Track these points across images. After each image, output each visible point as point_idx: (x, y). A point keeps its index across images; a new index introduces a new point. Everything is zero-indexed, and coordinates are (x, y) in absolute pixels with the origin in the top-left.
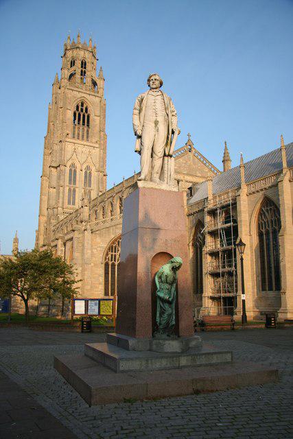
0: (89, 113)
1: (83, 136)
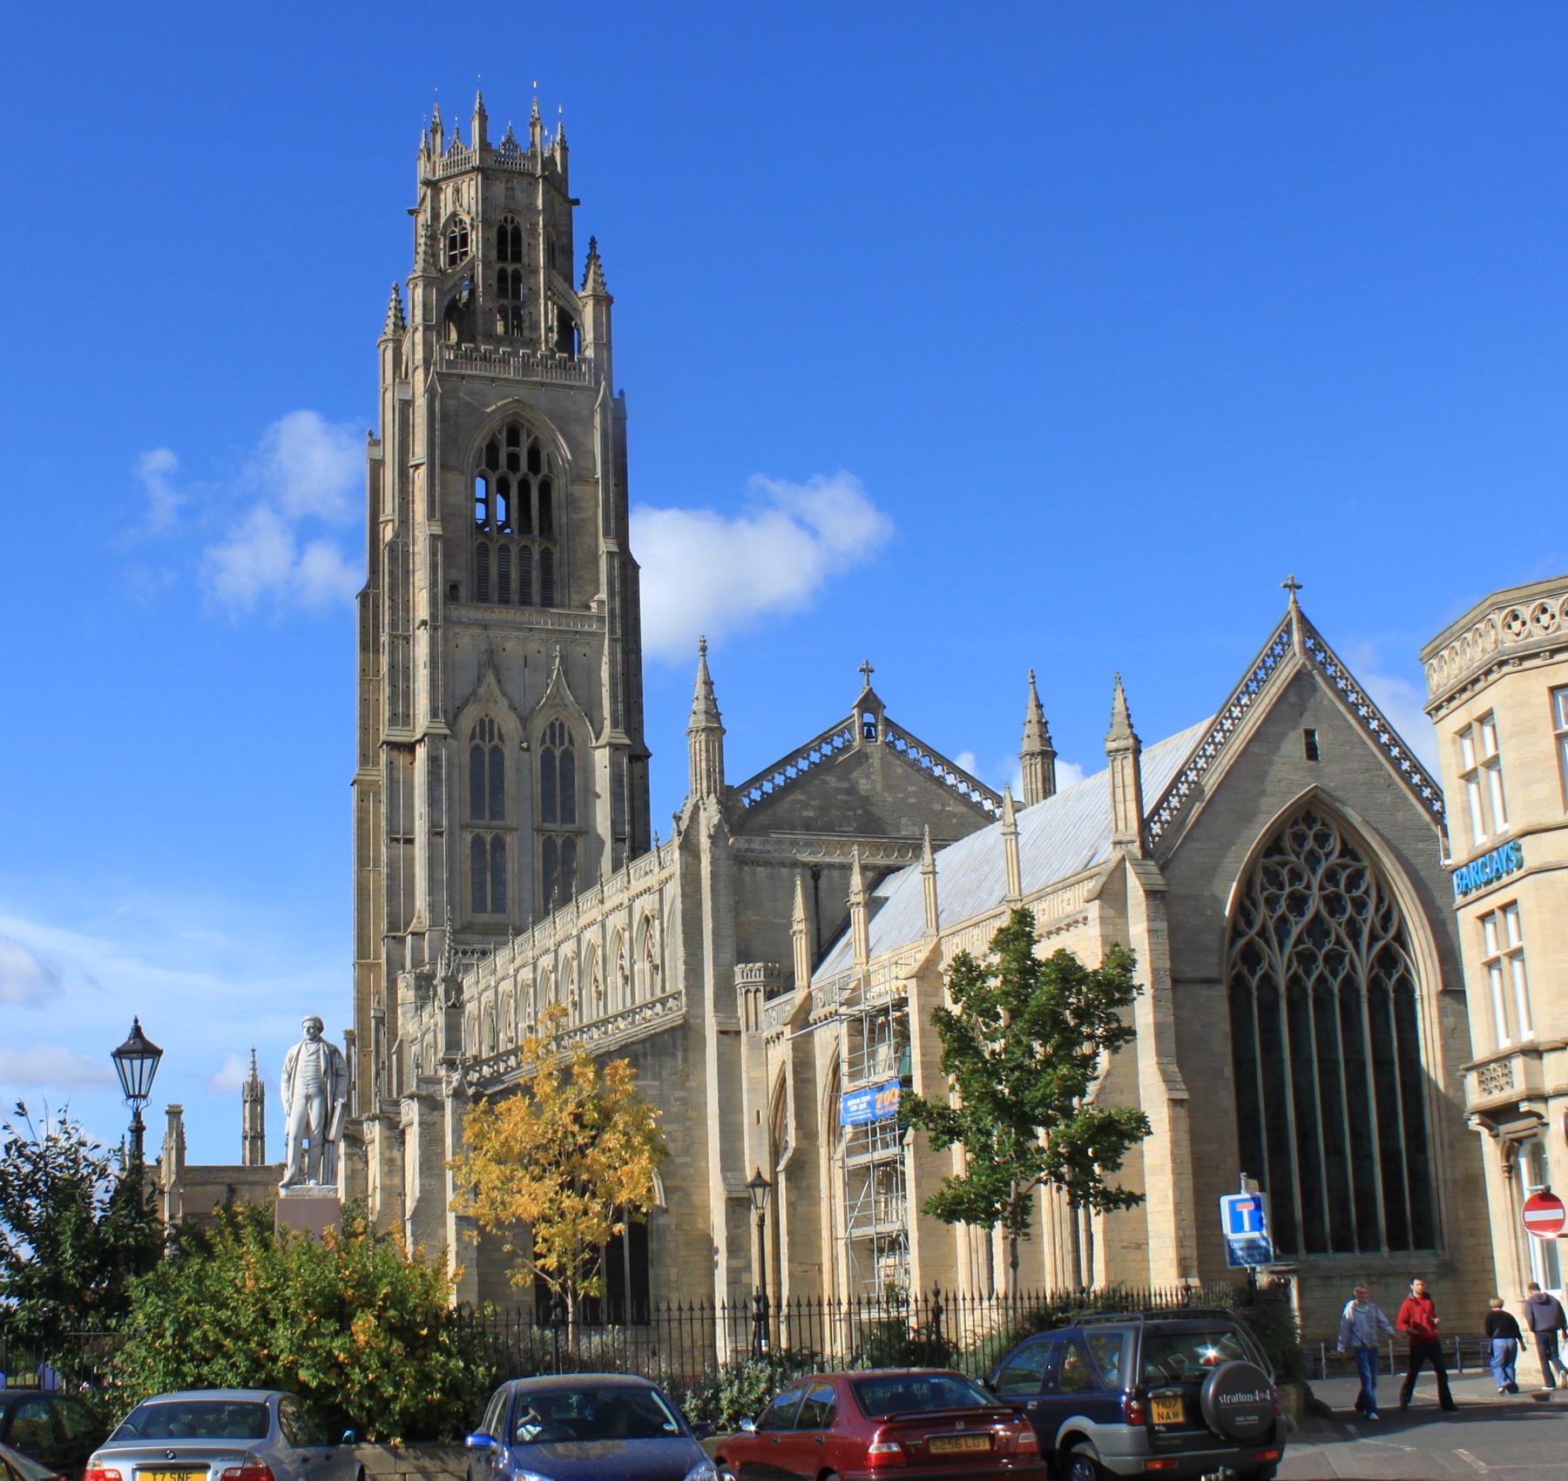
0: (545, 470)
1: (525, 582)
